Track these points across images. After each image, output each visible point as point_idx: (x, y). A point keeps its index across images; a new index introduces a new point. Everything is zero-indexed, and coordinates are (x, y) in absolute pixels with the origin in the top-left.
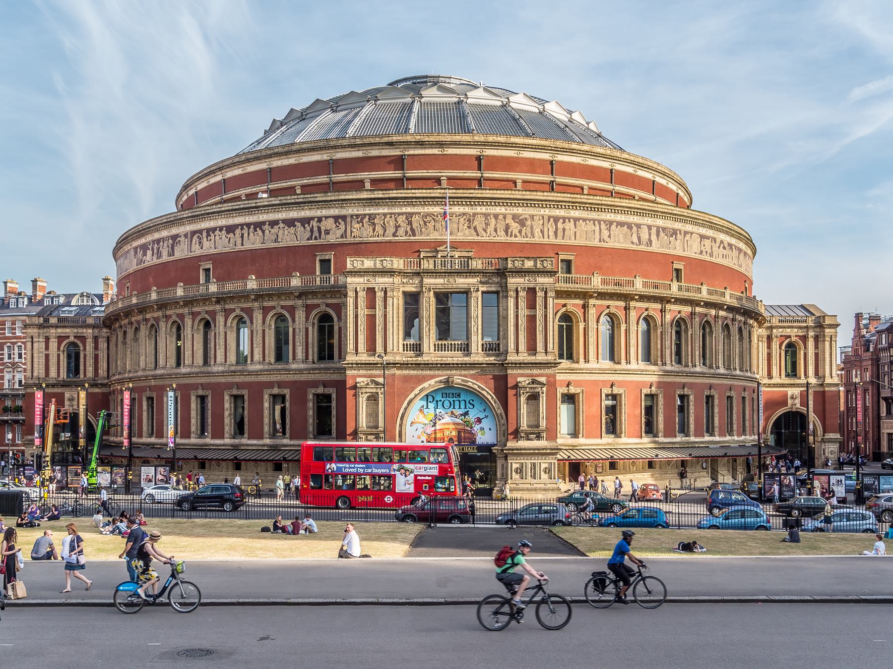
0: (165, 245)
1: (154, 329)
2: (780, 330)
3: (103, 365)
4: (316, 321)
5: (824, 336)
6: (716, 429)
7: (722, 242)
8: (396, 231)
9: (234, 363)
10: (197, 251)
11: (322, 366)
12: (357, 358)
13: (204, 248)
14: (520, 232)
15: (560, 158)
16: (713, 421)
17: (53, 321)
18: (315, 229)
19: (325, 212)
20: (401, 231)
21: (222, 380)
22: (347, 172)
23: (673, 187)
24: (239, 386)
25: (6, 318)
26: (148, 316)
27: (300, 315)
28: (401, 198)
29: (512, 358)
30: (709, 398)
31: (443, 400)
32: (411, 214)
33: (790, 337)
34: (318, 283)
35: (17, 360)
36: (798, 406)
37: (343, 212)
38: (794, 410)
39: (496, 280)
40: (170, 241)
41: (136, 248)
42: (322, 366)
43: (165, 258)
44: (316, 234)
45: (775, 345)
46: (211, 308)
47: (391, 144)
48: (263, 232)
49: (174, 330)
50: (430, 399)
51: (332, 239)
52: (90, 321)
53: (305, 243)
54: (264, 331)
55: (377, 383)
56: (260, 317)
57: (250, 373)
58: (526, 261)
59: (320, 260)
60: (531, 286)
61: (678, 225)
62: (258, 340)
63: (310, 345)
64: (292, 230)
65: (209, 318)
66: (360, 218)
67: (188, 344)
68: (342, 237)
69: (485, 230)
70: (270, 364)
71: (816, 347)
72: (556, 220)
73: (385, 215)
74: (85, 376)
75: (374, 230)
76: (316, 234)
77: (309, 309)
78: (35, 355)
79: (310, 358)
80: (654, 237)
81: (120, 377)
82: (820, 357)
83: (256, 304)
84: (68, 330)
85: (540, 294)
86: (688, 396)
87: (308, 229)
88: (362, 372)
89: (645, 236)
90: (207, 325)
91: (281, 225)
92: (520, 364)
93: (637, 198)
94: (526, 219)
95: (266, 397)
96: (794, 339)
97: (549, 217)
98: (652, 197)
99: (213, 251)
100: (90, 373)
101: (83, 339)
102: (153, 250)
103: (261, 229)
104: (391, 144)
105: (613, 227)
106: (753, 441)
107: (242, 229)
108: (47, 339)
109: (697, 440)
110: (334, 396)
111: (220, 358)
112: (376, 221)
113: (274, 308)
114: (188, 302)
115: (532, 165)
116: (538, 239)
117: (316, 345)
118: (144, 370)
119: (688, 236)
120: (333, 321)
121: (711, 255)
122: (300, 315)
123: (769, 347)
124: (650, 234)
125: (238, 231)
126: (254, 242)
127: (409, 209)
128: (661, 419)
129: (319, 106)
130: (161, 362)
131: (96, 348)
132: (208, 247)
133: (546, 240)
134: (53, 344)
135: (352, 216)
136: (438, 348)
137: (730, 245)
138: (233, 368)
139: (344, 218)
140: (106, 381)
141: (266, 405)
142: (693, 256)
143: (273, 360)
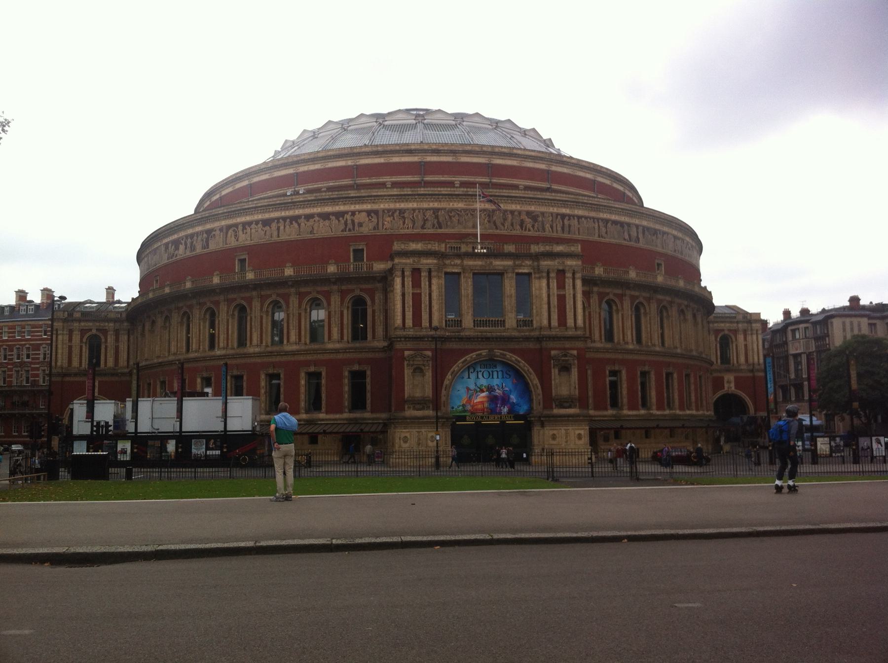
0: (200, 238)
1: (187, 318)
3: (123, 356)
4: (350, 305)
5: (752, 330)
6: (694, 404)
8: (424, 224)
9: (269, 344)
10: (232, 243)
11: (357, 345)
12: (405, 333)
13: (240, 240)
14: (533, 226)
15: (554, 168)
16: (690, 396)
17: (77, 315)
18: (349, 222)
19: (358, 207)
20: (429, 224)
21: (259, 360)
22: (370, 177)
24: (275, 364)
25: (15, 323)
26: (180, 305)
27: (335, 299)
28: (429, 195)
29: (546, 333)
30: (688, 376)
31: (483, 370)
32: (438, 210)
33: (723, 330)
34: (351, 269)
35: (26, 360)
36: (733, 388)
37: (375, 207)
39: (528, 263)
40: (205, 235)
41: (167, 245)
42: (357, 345)
43: (199, 250)
44: (350, 226)
46: (247, 295)
47: (410, 152)
48: (299, 225)
49: (208, 316)
50: (472, 370)
51: (366, 230)
52: (112, 316)
53: (339, 234)
54: (300, 314)
55: (425, 356)
56: (296, 302)
57: (287, 353)
58: (555, 246)
59: (355, 251)
60: (561, 268)
61: (658, 227)
62: (294, 323)
63: (345, 326)
64: (327, 223)
65: (245, 304)
66: (391, 212)
67: (223, 328)
68: (374, 228)
69: (503, 225)
70: (306, 344)
71: (745, 339)
72: (563, 216)
73: (414, 210)
74: (106, 365)
75: (404, 223)
76: (350, 226)
77: (343, 294)
78: (60, 346)
79: (345, 338)
80: (641, 236)
81: (147, 363)
82: (750, 347)
83: (293, 290)
84: (91, 324)
85: (569, 275)
86: (671, 374)
87: (343, 222)
88: (409, 345)
89: (634, 233)
90: (242, 309)
91: (317, 218)
92: (554, 338)
94: (538, 216)
95: (303, 375)
96: (726, 332)
97: (557, 214)
99: (248, 243)
100: (111, 363)
101: (105, 332)
102: (186, 244)
103: (297, 222)
104: (410, 152)
105: (609, 224)
106: (709, 416)
107: (278, 222)
108: (71, 332)
109: (681, 413)
110: (368, 373)
111: (255, 341)
112: (406, 215)
113: (310, 293)
114: (225, 290)
115: (532, 174)
116: (548, 233)
117: (350, 326)
118: (175, 354)
120: (365, 303)
121: (682, 253)
122: (335, 299)
125: (274, 225)
126: (290, 233)
127: (436, 205)
128: (653, 394)
129: (331, 126)
130: (194, 346)
131: (117, 340)
132: (244, 239)
133: (555, 235)
134: (76, 338)
135: (383, 211)
136: (476, 323)
137: (692, 246)
138: (269, 349)
139: (376, 212)
140: (126, 370)
141: (303, 382)
143: (308, 341)
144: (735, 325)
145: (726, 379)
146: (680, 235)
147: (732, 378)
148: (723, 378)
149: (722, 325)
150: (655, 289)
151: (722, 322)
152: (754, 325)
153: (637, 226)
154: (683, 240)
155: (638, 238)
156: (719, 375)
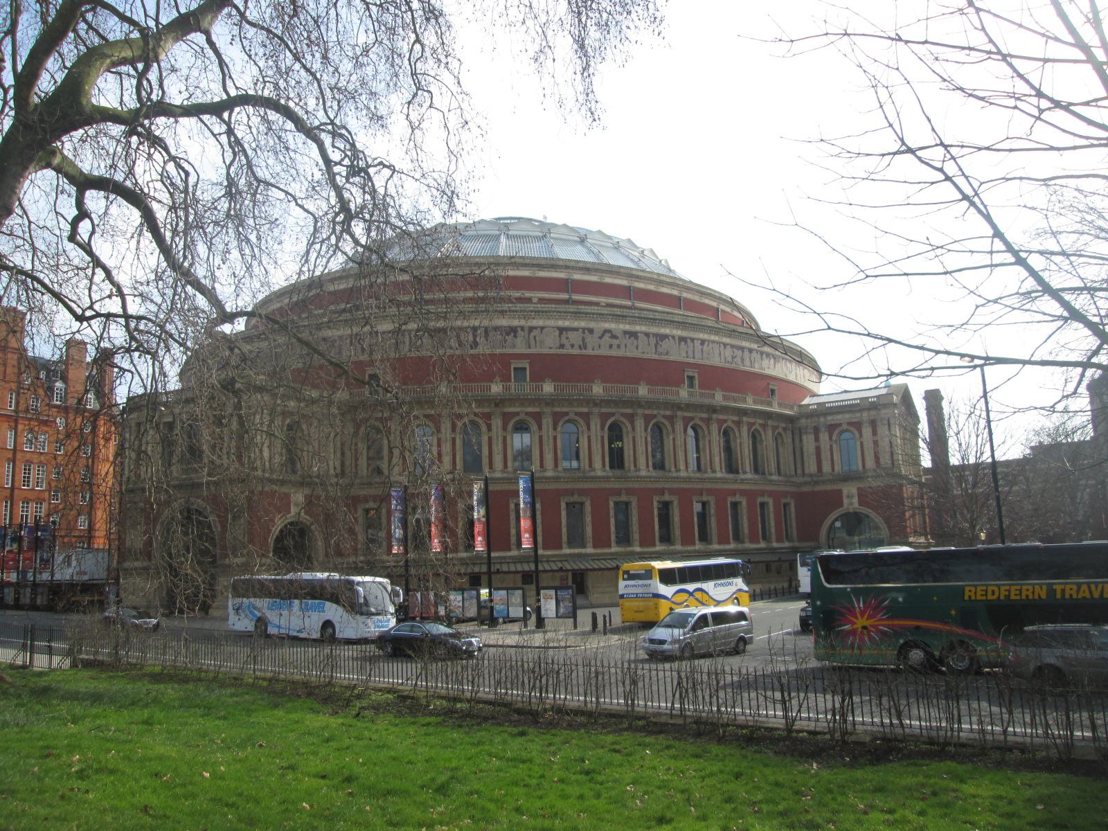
2: (829, 418)
7: (606, 331)
23: (624, 282)
33: (840, 425)
36: (856, 505)
38: (851, 511)
45: (824, 437)
61: (516, 323)
71: (875, 433)
93: (535, 300)
94: (335, 341)
96: (845, 427)
98: (565, 296)
119: (534, 333)
123: (817, 439)
124: (475, 336)
142: (545, 351)
144: (858, 415)
145: (845, 492)
146: (583, 324)
147: (855, 491)
148: (840, 492)
149: (839, 417)
150: (499, 402)
151: (838, 413)
152: (883, 411)
153: (475, 329)
154: (591, 331)
155: (475, 344)
156: (835, 487)
